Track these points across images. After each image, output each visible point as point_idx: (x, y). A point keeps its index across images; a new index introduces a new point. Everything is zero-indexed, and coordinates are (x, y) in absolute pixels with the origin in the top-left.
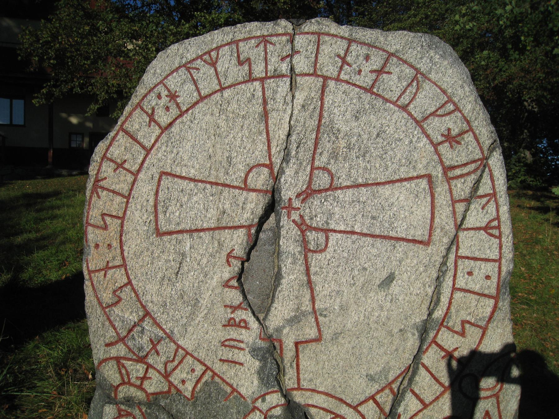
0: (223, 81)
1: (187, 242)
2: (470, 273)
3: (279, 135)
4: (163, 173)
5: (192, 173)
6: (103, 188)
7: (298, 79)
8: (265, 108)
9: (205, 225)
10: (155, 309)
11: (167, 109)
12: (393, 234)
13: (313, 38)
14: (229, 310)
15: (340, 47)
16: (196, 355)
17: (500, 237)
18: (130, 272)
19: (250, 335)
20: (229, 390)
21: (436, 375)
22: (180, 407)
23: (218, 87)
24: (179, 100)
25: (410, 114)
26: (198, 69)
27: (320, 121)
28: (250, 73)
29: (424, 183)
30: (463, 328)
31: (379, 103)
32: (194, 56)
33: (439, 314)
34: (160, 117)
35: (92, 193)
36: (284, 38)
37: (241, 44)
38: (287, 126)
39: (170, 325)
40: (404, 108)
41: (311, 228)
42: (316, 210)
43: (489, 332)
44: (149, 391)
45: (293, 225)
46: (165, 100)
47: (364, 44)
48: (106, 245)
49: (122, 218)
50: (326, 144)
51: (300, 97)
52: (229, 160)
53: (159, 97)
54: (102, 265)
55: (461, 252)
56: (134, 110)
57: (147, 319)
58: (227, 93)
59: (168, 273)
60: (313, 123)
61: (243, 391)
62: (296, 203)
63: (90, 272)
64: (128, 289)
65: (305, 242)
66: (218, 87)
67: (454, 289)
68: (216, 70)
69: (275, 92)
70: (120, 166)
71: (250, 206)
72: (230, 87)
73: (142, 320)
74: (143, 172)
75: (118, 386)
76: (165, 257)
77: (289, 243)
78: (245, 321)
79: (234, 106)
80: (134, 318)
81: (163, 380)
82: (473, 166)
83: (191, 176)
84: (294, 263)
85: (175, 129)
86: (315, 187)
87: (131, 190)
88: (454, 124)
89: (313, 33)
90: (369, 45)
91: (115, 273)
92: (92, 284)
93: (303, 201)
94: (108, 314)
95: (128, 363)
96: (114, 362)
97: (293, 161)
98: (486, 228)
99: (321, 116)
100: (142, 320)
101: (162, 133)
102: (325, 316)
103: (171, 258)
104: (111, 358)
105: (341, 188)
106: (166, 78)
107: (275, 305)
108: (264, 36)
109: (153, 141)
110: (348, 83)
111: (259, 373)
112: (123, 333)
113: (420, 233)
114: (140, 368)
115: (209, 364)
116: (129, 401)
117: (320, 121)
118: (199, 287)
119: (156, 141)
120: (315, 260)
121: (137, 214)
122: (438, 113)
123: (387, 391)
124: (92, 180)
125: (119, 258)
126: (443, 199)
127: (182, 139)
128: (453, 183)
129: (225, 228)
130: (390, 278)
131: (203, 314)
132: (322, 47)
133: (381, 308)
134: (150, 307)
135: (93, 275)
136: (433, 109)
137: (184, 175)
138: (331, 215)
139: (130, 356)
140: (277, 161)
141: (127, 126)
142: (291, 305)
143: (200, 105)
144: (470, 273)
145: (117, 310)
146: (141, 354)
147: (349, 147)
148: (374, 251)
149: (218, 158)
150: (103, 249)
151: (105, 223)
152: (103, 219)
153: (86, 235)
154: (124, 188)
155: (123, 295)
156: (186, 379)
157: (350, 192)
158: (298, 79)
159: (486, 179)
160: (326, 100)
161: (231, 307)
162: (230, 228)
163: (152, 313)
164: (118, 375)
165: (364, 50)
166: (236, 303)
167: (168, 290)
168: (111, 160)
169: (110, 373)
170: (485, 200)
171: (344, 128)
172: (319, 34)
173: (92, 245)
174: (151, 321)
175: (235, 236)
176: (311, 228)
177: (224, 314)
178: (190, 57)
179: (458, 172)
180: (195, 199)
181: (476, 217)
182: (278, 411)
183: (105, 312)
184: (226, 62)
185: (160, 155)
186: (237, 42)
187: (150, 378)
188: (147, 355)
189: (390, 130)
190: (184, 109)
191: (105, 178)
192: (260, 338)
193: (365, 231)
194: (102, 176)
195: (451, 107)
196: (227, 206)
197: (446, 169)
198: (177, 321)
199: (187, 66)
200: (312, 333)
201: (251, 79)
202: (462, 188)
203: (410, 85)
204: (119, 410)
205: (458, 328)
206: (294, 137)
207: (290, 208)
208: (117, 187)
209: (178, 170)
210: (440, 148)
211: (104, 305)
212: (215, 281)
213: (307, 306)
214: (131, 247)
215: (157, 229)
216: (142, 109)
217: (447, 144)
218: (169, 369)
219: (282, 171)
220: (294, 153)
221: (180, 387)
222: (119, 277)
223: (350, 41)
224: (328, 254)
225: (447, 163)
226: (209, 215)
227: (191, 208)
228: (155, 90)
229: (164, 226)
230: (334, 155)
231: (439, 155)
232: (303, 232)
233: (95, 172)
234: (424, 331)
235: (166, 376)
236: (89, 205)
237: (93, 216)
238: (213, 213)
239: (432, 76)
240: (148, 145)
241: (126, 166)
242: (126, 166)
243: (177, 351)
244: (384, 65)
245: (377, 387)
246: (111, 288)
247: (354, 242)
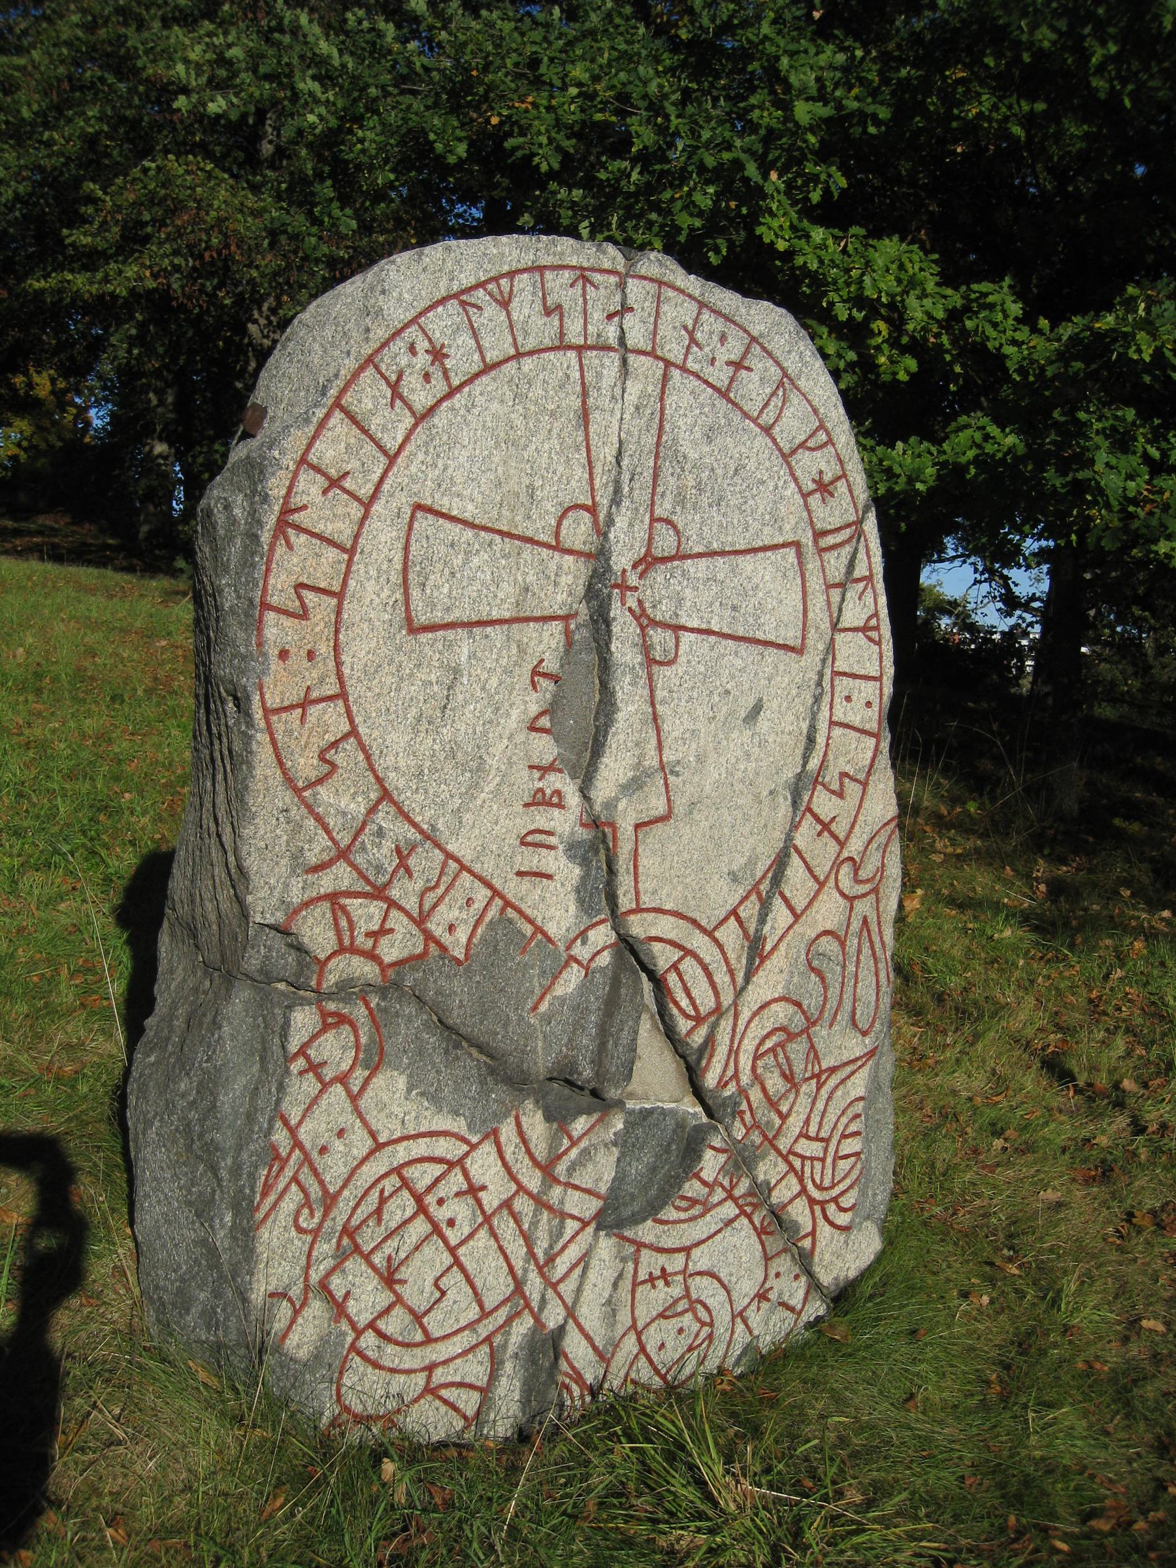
0: (520, 339)
1: (464, 646)
2: (848, 699)
3: (605, 453)
4: (418, 507)
5: (471, 512)
6: (299, 529)
7: (631, 358)
8: (584, 403)
9: (495, 614)
10: (401, 783)
11: (427, 377)
12: (760, 635)
13: (652, 288)
14: (537, 774)
15: (688, 312)
16: (477, 868)
17: (879, 643)
18: (354, 709)
19: (564, 822)
20: (528, 930)
21: (812, 863)
22: (442, 982)
23: (512, 352)
24: (449, 363)
25: (774, 440)
26: (479, 308)
27: (659, 437)
28: (562, 335)
29: (791, 553)
30: (842, 784)
31: (737, 417)
32: (472, 281)
33: (814, 763)
34: (413, 390)
35: (275, 537)
36: (613, 279)
37: (549, 275)
38: (615, 440)
39: (429, 813)
40: (767, 430)
41: (655, 623)
42: (663, 591)
43: (870, 789)
44: (387, 959)
45: (629, 618)
46: (423, 360)
47: (718, 313)
48: (303, 653)
49: (340, 596)
50: (669, 482)
51: (634, 389)
52: (531, 489)
53: (412, 350)
54: (294, 696)
55: (841, 666)
56: (362, 368)
57: (384, 806)
58: (528, 364)
59: (428, 710)
60: (650, 440)
61: (552, 929)
62: (633, 579)
63: (268, 712)
64: (350, 744)
65: (646, 649)
66: (512, 352)
67: (832, 723)
68: (509, 315)
69: (599, 375)
70: (334, 483)
71: (566, 580)
72: (531, 353)
73: (372, 810)
74: (383, 501)
75: (329, 958)
76: (421, 675)
77: (624, 649)
78: (558, 793)
79: (537, 391)
80: (358, 808)
81: (415, 931)
82: (846, 533)
83: (467, 516)
84: (633, 684)
85: (440, 420)
86: (658, 553)
87: (357, 537)
89: (651, 280)
90: (727, 318)
91: (325, 712)
92: (274, 742)
93: (642, 576)
94: (311, 801)
95: (352, 904)
96: (326, 906)
97: (626, 503)
98: (864, 629)
99: (661, 428)
100: (372, 810)
101: (416, 425)
102: (677, 775)
103: (433, 678)
104: (320, 898)
105: (690, 557)
106: (421, 314)
107: (605, 760)
108: (582, 269)
109: (400, 440)
110: (698, 377)
111: (578, 891)
112: (344, 839)
113: (791, 636)
114: (376, 908)
115: (497, 883)
116: (347, 989)
117: (659, 437)
118: (485, 734)
119: (407, 439)
120: (664, 675)
121: (371, 586)
122: (810, 444)
123: (753, 897)
124: (277, 508)
125: (333, 679)
126: (815, 583)
127: (454, 442)
128: (826, 556)
129: (527, 620)
130: (757, 709)
131: (491, 787)
132: (665, 308)
133: (748, 755)
134: (394, 780)
135: (275, 718)
136: (803, 438)
137: (455, 513)
138: (680, 601)
139: (361, 886)
140: (604, 501)
141: (347, 400)
142: (629, 759)
143: (485, 379)
144: (848, 699)
145: (324, 793)
146: (382, 880)
147: (699, 487)
148: (739, 663)
149: (512, 485)
150: (297, 660)
151: (303, 605)
152: (300, 598)
153: (260, 630)
154: (343, 530)
155: (339, 758)
157: (703, 563)
158: (631, 358)
159: (862, 555)
160: (668, 402)
161: (538, 768)
162: (536, 619)
163: (395, 794)
164: (331, 934)
165: (719, 325)
166: (547, 759)
167: (427, 743)
168: (317, 469)
169: (317, 932)
170: (862, 585)
171: (693, 455)
172: (661, 283)
173: (273, 652)
174: (392, 809)
175: (546, 634)
176: (655, 623)
178: (467, 280)
179: (830, 540)
180: (476, 561)
182: (605, 959)
183: (303, 800)
184: (525, 307)
185: (413, 469)
186: (541, 269)
187: (391, 931)
188: (390, 881)
189: (751, 465)
190: (456, 382)
191: (305, 507)
192: (582, 825)
193: (726, 630)
194: (296, 501)
195: (822, 437)
196: (531, 578)
197: (819, 535)
198: (443, 804)
199: (461, 297)
200: (658, 806)
201: (562, 346)
202: (836, 564)
203: (774, 394)
204: (324, 1014)
205: (835, 786)
206: (625, 463)
207: (624, 587)
208: (328, 529)
209: (444, 503)
210: (810, 500)
211: (300, 784)
212: (514, 719)
213: (651, 760)
214: (357, 654)
215: (409, 619)
216: (376, 367)
217: (818, 495)
218: (427, 907)
219: (610, 522)
220: (626, 489)
221: (446, 939)
222: (332, 719)
223: (702, 305)
224: (679, 668)
225: (819, 526)
226: (501, 595)
227: (472, 579)
228: (406, 334)
229: (422, 617)
230: (681, 500)
231: (809, 511)
232: (643, 628)
233: (283, 492)
234: (800, 788)
235: (420, 920)
236: (269, 562)
237: (280, 588)
238: (507, 590)
239: (802, 383)
240: (392, 445)
241: (348, 484)
242: (348, 484)
243: (444, 865)
244: (744, 357)
245: (741, 892)
246: (318, 743)
247: (712, 649)
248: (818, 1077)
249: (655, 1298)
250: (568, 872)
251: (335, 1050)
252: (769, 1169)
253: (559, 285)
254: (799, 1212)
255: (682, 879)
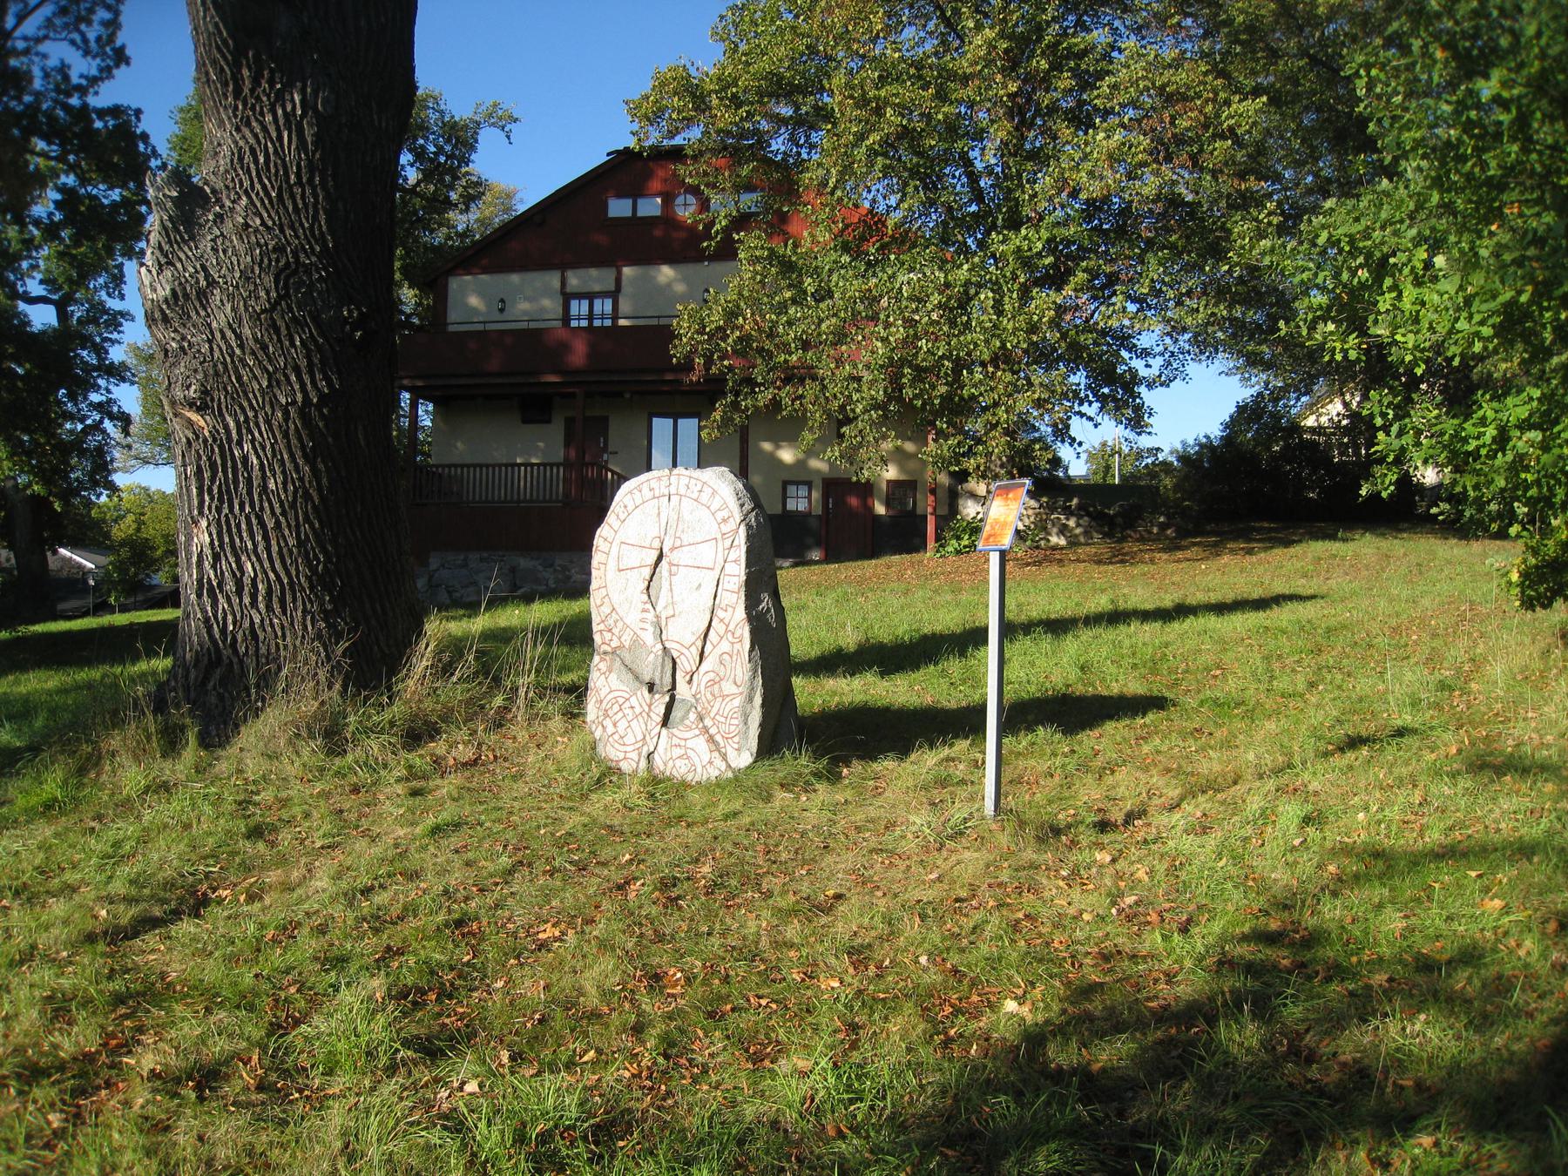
19: (650, 616)
88: (725, 514)
156: (627, 640)
177: (641, 606)
181: (733, 555)
184: (645, 489)
202: (728, 543)
248: (724, 697)
249: (678, 752)
250: (651, 629)
251: (603, 666)
252: (708, 722)
253: (654, 484)
254: (718, 738)
255: (682, 635)
